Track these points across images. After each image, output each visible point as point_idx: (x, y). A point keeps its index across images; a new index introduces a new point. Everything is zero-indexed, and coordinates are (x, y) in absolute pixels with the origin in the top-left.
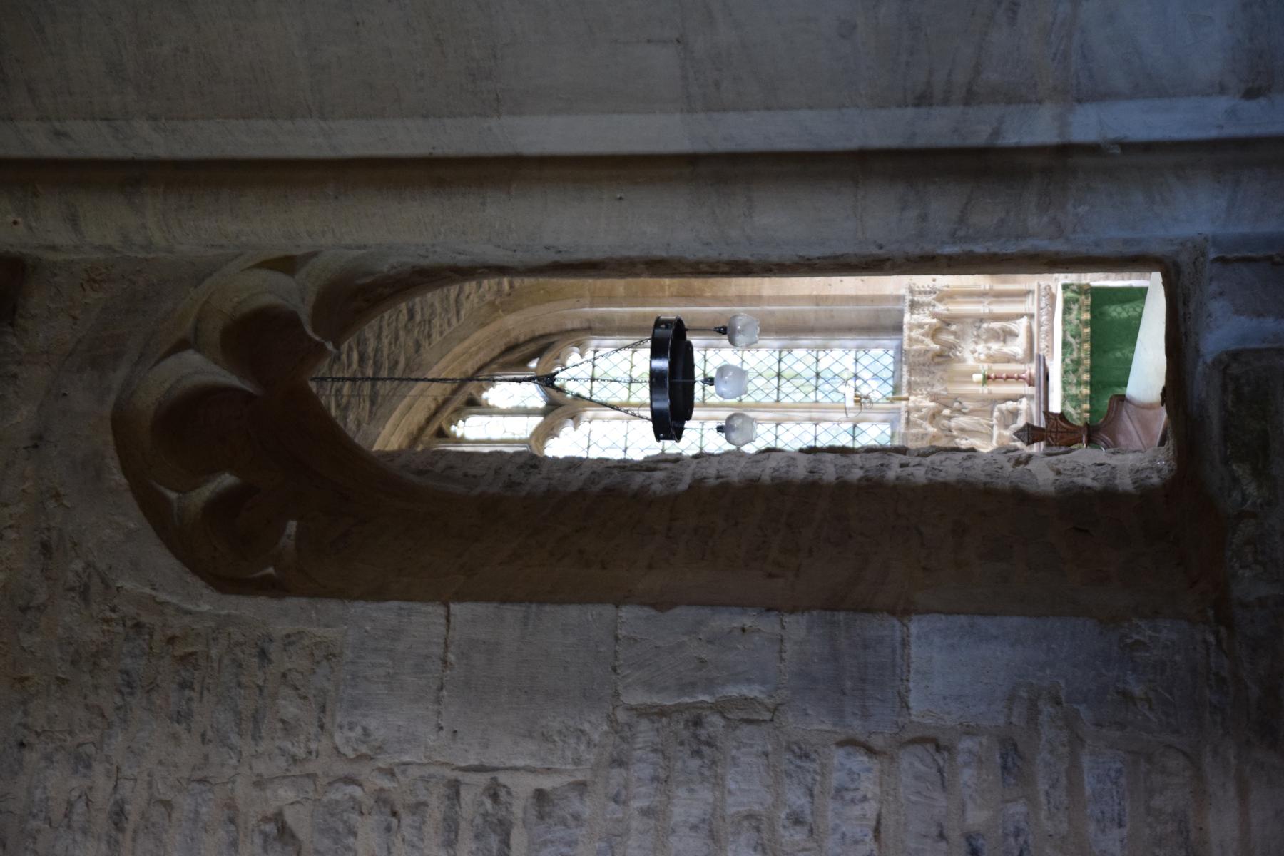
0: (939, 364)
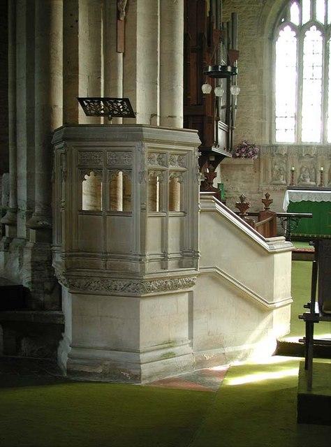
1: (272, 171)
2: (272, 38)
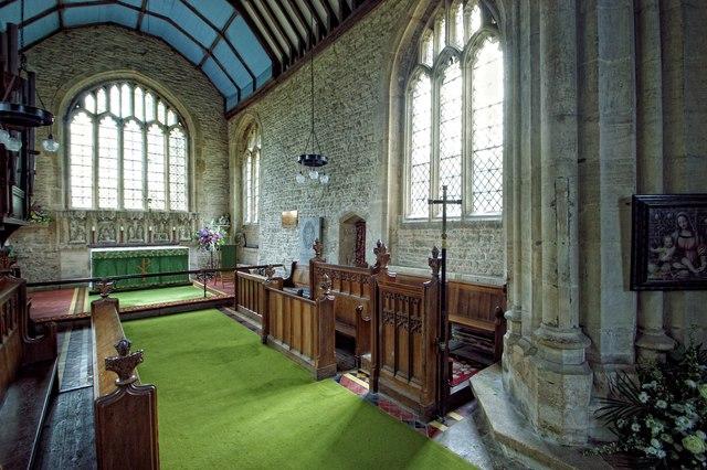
2: (67, 119)
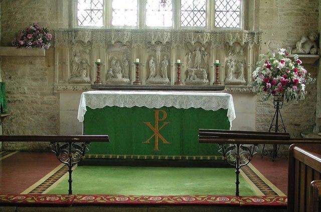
0: (225, 46)
1: (71, 65)
